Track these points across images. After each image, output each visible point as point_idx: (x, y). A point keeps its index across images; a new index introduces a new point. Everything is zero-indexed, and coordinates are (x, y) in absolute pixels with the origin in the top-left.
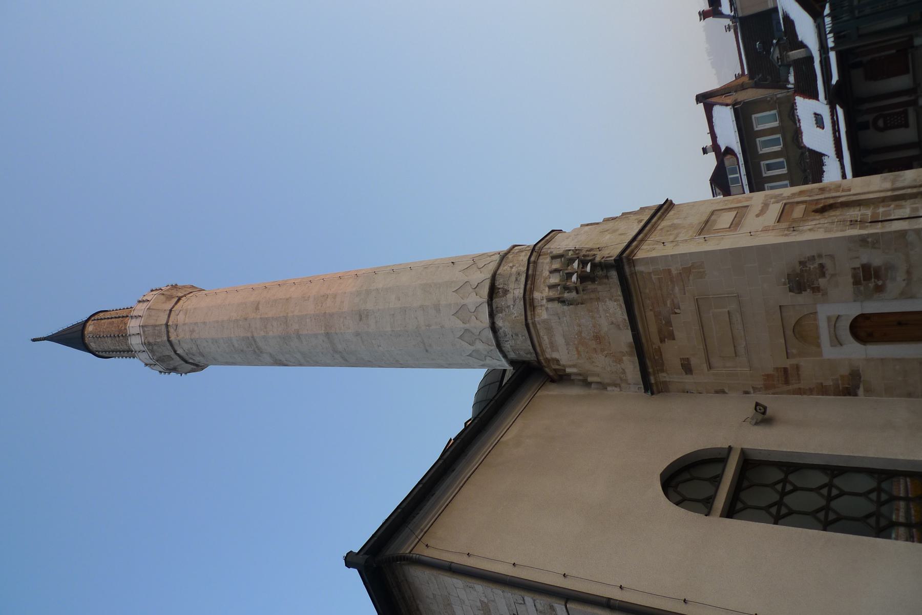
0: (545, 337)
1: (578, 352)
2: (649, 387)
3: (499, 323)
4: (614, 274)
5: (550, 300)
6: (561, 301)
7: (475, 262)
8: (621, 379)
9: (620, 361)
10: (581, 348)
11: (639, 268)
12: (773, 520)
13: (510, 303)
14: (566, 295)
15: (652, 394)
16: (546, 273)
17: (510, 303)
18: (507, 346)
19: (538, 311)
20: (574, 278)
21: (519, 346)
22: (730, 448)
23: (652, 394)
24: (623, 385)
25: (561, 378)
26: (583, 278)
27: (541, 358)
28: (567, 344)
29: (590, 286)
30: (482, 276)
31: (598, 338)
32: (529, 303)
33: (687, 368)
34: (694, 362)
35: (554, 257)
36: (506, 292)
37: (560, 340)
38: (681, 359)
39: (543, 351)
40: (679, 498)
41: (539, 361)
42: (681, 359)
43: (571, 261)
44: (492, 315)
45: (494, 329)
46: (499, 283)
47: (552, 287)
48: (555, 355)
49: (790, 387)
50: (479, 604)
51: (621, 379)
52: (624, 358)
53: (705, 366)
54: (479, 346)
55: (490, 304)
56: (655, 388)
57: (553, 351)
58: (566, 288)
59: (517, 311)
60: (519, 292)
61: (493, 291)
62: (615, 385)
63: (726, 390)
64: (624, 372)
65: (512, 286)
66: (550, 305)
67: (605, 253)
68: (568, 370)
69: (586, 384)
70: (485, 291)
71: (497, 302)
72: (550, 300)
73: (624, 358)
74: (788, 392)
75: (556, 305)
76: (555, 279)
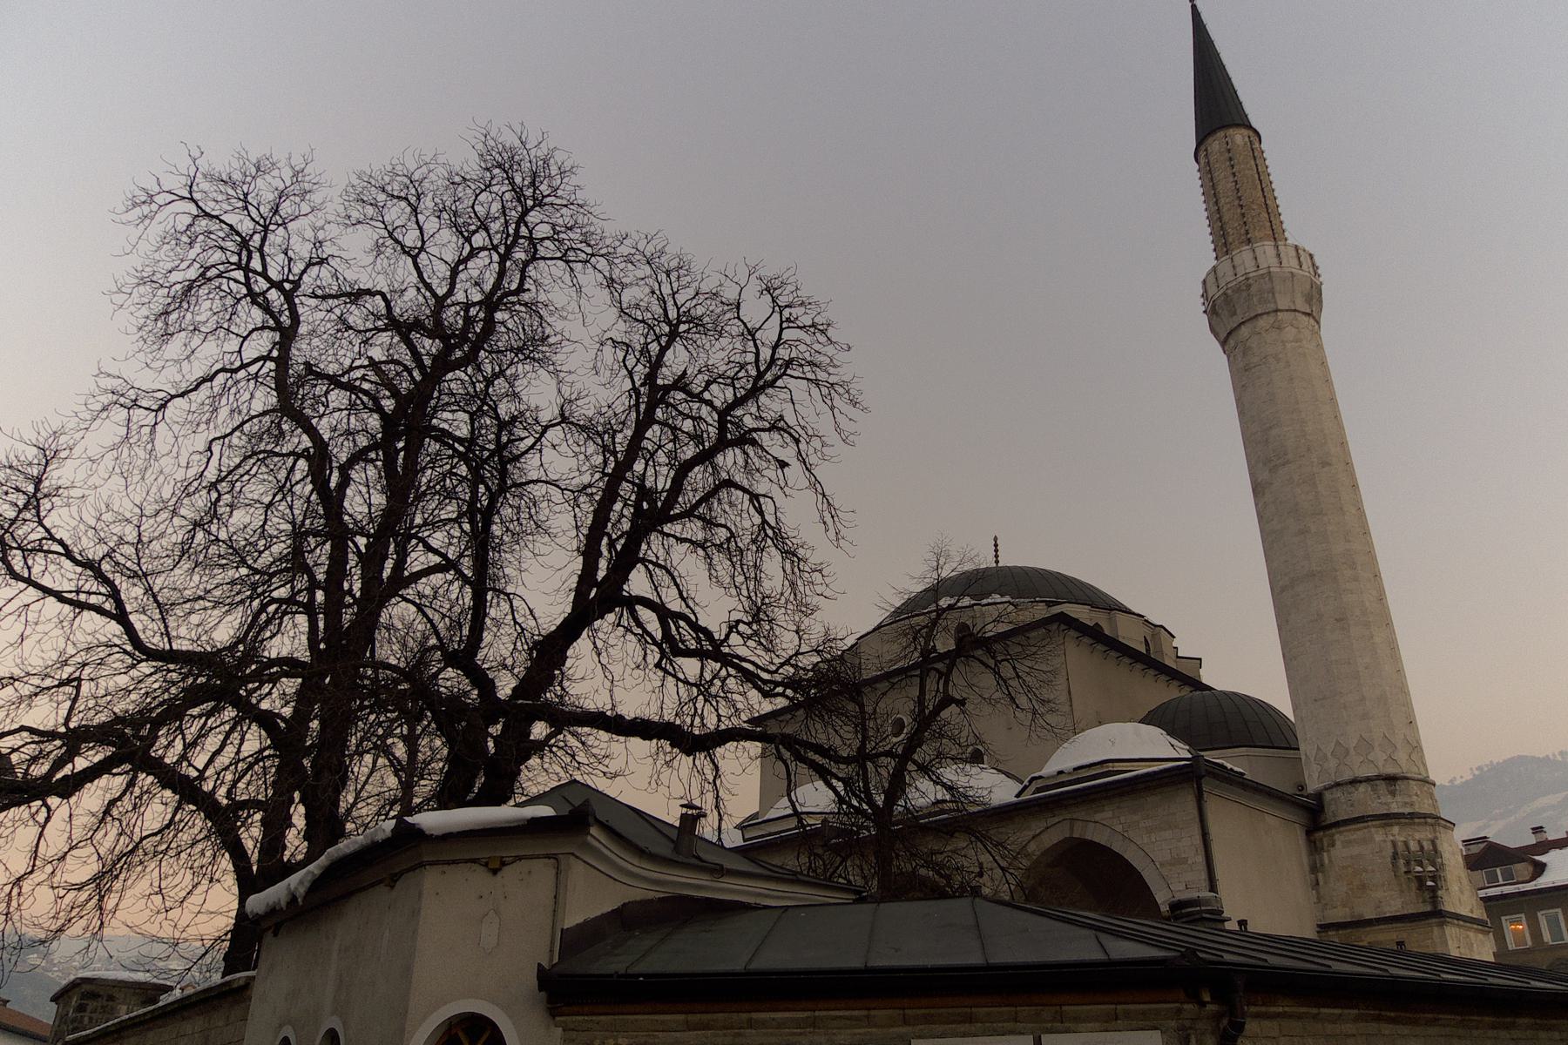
1: (1344, 868)
3: (1362, 788)
4: (1428, 908)
5: (1394, 844)
6: (1395, 856)
7: (1416, 748)
11: (1436, 930)
13: (1383, 799)
14: (1402, 861)
16: (1417, 836)
17: (1383, 799)
18: (1337, 793)
19: (1381, 831)
20: (1419, 869)
21: (1338, 806)
25: (1315, 848)
26: (1420, 880)
29: (1414, 885)
30: (1403, 765)
31: (1363, 887)
32: (1388, 818)
35: (1433, 842)
36: (1393, 794)
37: (1356, 850)
43: (1433, 864)
44: (1368, 780)
45: (1354, 782)
46: (1400, 785)
47: (1406, 843)
48: (1338, 844)
54: (1332, 764)
55: (1379, 777)
58: (1408, 863)
59: (1376, 808)
60: (1395, 809)
61: (1391, 779)
62: (1319, 899)
65: (1398, 798)
66: (1389, 845)
67: (1445, 898)
69: (1314, 869)
70: (1390, 770)
71: (1382, 785)
72: (1394, 844)
75: (1390, 851)
76: (1413, 846)
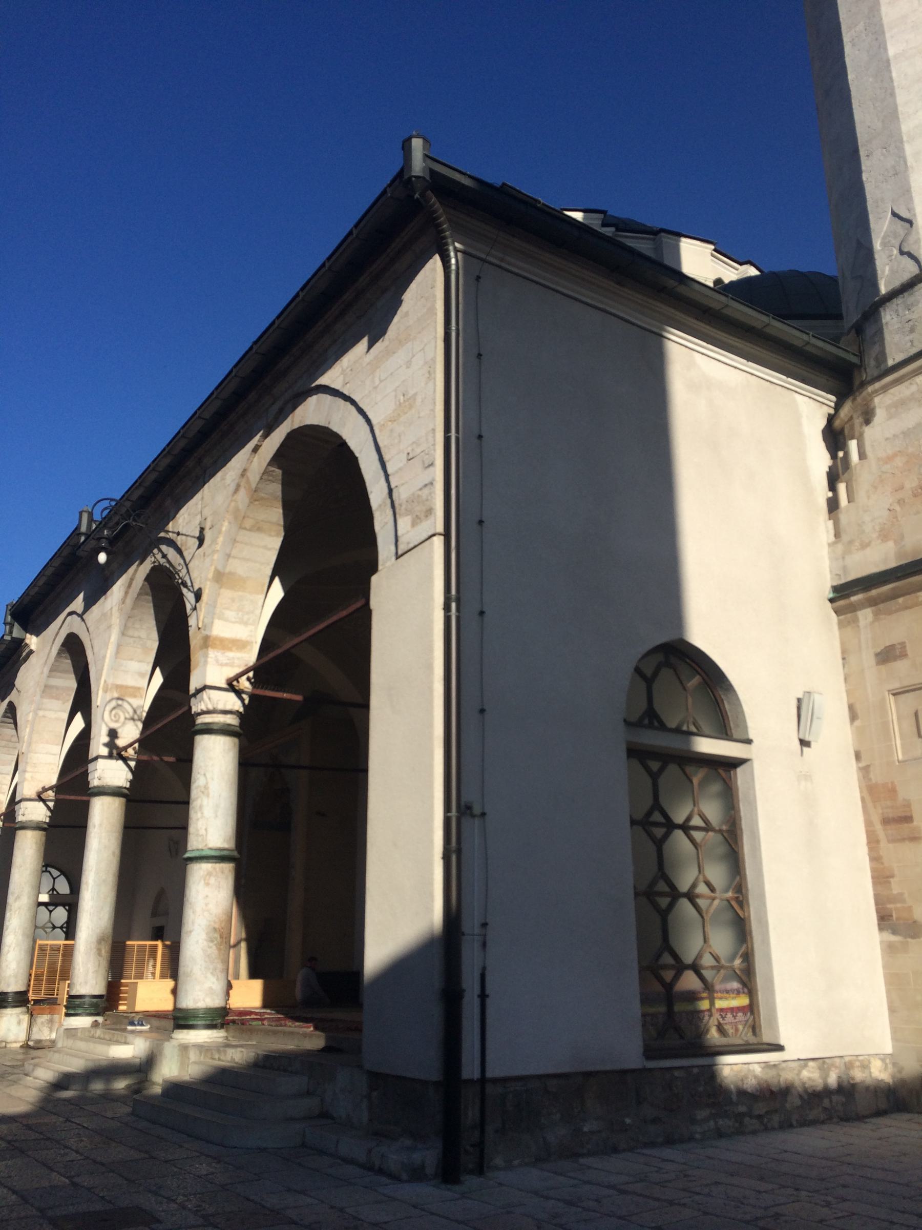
0: (914, 388)
2: (845, 594)
8: (851, 542)
9: (884, 536)
10: (899, 462)
12: (639, 816)
15: (831, 600)
22: (749, 742)
23: (831, 600)
24: (840, 548)
27: (870, 389)
28: (906, 434)
33: (887, 656)
34: (901, 666)
38: (903, 644)
39: (885, 389)
40: (649, 672)
41: (863, 385)
42: (903, 644)
49: (878, 827)
50: (411, 392)
51: (851, 542)
52: (891, 544)
53: (896, 685)
56: (841, 603)
57: (888, 408)
62: (837, 535)
63: (857, 723)
64: (864, 546)
68: (853, 445)
73: (891, 544)
74: (868, 824)
